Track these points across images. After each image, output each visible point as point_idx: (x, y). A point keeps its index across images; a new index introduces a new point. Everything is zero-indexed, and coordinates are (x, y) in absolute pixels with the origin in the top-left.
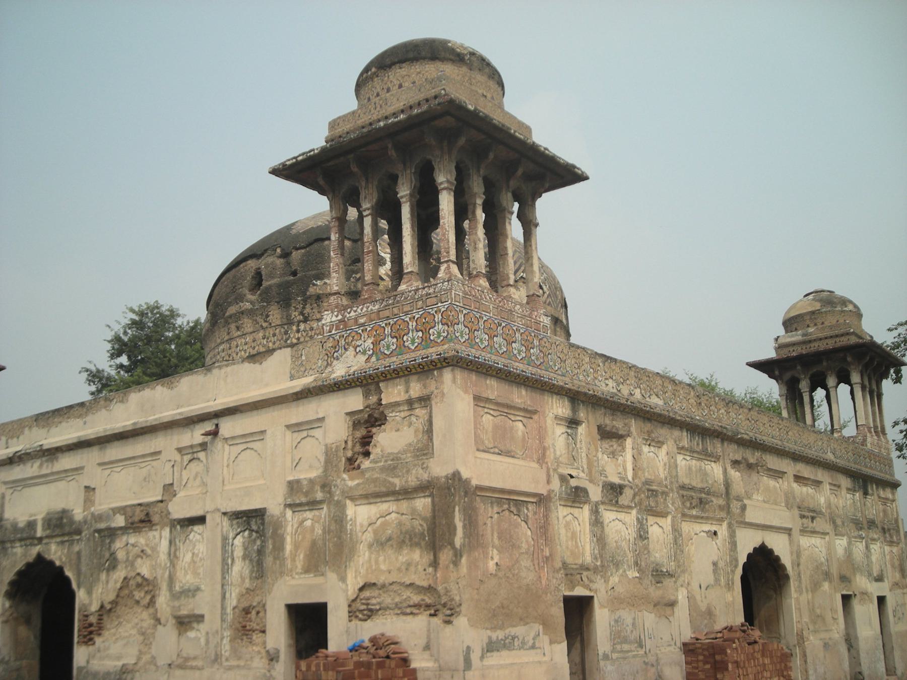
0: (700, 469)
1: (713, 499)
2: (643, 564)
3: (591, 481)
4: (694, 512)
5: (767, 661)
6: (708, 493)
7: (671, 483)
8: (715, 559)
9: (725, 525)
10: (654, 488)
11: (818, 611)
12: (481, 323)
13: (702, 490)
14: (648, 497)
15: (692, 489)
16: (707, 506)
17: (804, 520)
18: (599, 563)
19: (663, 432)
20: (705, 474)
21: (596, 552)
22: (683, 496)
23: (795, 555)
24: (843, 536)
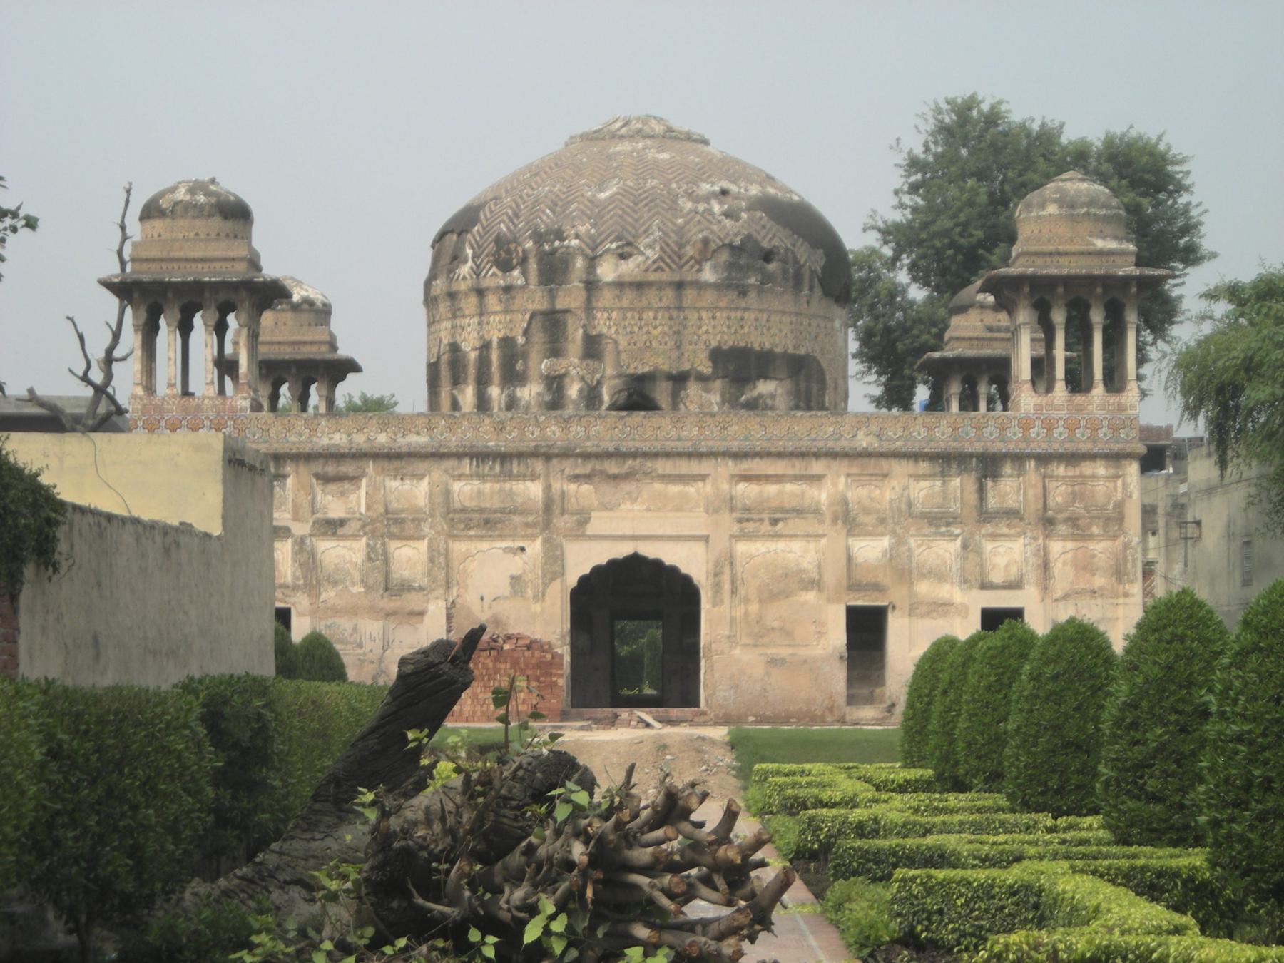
0: (500, 490)
1: (513, 517)
2: (371, 581)
3: (296, 518)
4: (472, 533)
5: (503, 666)
6: (510, 513)
7: (432, 509)
8: (517, 572)
9: (539, 541)
10: (403, 516)
11: (775, 624)
12: (163, 423)
13: (502, 511)
14: (388, 525)
15: (481, 511)
16: (499, 526)
17: (745, 524)
18: (301, 582)
19: (420, 466)
20: (511, 493)
21: (299, 573)
22: (452, 520)
23: (711, 565)
24: (883, 535)
